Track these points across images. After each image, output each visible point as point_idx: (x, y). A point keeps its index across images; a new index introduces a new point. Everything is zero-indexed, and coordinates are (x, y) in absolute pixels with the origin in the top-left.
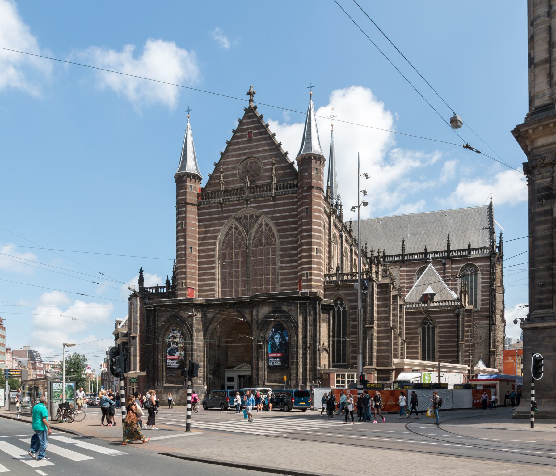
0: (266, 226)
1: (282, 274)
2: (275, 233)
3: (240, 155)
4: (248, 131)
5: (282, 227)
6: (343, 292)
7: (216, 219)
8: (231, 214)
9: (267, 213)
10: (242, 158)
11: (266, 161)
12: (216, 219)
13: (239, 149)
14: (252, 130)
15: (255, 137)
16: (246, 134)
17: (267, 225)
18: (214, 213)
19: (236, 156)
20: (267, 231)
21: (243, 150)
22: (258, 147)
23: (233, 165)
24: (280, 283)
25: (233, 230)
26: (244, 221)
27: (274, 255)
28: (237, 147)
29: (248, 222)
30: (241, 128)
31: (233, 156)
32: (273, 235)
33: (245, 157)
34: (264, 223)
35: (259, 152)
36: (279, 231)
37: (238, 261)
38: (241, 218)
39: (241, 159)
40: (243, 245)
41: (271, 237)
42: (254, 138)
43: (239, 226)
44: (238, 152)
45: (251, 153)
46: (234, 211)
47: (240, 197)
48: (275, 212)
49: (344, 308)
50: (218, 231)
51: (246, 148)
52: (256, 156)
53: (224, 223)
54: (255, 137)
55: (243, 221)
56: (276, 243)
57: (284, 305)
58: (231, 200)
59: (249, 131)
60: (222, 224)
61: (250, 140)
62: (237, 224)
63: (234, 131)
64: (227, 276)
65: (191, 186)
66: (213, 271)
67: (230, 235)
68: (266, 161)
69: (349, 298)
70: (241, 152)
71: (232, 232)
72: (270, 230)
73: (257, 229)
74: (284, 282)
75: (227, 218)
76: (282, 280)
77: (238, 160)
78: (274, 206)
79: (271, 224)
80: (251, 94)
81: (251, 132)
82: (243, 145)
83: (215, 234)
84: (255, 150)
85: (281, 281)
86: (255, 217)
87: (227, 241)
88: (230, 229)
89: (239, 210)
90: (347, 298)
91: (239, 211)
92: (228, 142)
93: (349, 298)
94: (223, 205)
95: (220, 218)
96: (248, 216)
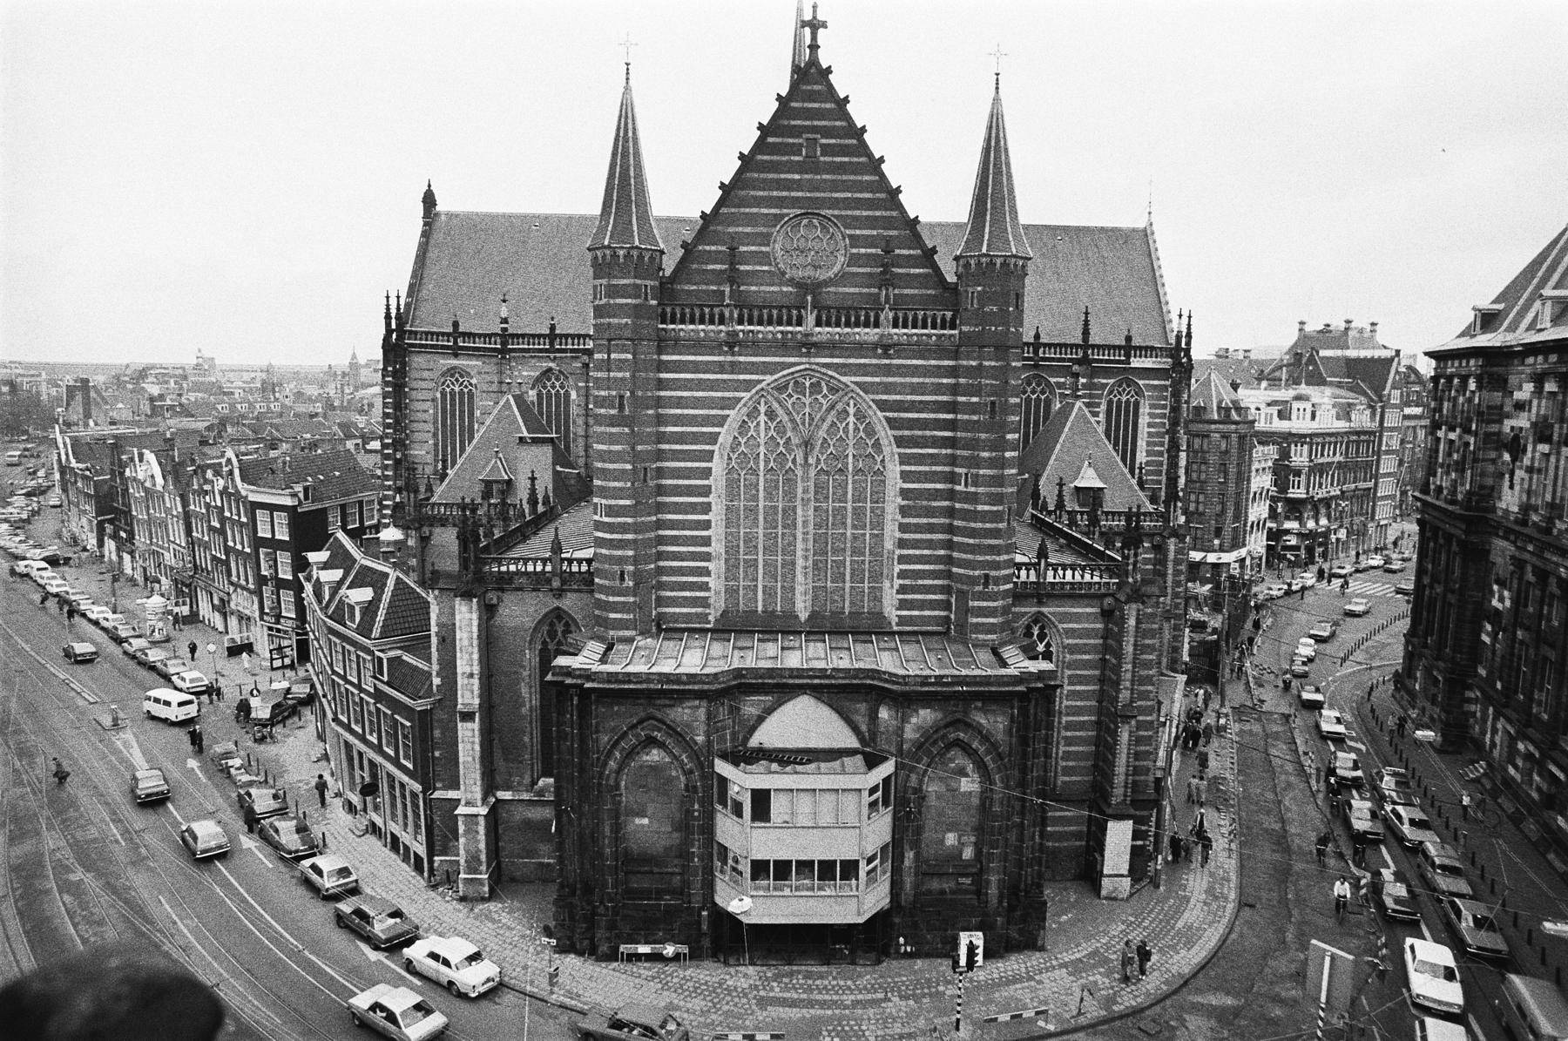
1: (902, 559)
2: (884, 442)
3: (780, 202)
5: (907, 433)
6: (1051, 609)
7: (713, 386)
8: (761, 377)
9: (866, 388)
10: (785, 211)
11: (858, 232)
12: (713, 386)
15: (827, 159)
16: (801, 145)
17: (860, 416)
20: (862, 434)
21: (789, 189)
22: (835, 186)
24: (898, 582)
25: (762, 418)
26: (793, 400)
27: (877, 502)
28: (771, 176)
31: (759, 202)
32: (877, 445)
34: (852, 410)
35: (835, 203)
37: (776, 508)
38: (786, 387)
39: (788, 215)
41: (870, 450)
42: (822, 159)
43: (780, 412)
47: (788, 332)
48: (888, 388)
49: (1048, 645)
50: (721, 420)
51: (798, 185)
52: (829, 212)
54: (827, 159)
55: (790, 396)
57: (976, 708)
59: (810, 136)
61: (811, 166)
62: (775, 405)
68: (858, 232)
69: (1065, 626)
70: (785, 194)
71: (758, 424)
72: (870, 432)
73: (833, 424)
74: (907, 582)
75: (748, 386)
76: (902, 575)
77: (775, 215)
78: (888, 370)
79: (878, 417)
80: (815, 25)
81: (815, 139)
83: (717, 429)
87: (743, 448)
88: (753, 413)
89: (783, 369)
90: (1060, 626)
91: (785, 372)
92: (742, 156)
93: (1065, 626)
94: (736, 349)
96: (808, 384)
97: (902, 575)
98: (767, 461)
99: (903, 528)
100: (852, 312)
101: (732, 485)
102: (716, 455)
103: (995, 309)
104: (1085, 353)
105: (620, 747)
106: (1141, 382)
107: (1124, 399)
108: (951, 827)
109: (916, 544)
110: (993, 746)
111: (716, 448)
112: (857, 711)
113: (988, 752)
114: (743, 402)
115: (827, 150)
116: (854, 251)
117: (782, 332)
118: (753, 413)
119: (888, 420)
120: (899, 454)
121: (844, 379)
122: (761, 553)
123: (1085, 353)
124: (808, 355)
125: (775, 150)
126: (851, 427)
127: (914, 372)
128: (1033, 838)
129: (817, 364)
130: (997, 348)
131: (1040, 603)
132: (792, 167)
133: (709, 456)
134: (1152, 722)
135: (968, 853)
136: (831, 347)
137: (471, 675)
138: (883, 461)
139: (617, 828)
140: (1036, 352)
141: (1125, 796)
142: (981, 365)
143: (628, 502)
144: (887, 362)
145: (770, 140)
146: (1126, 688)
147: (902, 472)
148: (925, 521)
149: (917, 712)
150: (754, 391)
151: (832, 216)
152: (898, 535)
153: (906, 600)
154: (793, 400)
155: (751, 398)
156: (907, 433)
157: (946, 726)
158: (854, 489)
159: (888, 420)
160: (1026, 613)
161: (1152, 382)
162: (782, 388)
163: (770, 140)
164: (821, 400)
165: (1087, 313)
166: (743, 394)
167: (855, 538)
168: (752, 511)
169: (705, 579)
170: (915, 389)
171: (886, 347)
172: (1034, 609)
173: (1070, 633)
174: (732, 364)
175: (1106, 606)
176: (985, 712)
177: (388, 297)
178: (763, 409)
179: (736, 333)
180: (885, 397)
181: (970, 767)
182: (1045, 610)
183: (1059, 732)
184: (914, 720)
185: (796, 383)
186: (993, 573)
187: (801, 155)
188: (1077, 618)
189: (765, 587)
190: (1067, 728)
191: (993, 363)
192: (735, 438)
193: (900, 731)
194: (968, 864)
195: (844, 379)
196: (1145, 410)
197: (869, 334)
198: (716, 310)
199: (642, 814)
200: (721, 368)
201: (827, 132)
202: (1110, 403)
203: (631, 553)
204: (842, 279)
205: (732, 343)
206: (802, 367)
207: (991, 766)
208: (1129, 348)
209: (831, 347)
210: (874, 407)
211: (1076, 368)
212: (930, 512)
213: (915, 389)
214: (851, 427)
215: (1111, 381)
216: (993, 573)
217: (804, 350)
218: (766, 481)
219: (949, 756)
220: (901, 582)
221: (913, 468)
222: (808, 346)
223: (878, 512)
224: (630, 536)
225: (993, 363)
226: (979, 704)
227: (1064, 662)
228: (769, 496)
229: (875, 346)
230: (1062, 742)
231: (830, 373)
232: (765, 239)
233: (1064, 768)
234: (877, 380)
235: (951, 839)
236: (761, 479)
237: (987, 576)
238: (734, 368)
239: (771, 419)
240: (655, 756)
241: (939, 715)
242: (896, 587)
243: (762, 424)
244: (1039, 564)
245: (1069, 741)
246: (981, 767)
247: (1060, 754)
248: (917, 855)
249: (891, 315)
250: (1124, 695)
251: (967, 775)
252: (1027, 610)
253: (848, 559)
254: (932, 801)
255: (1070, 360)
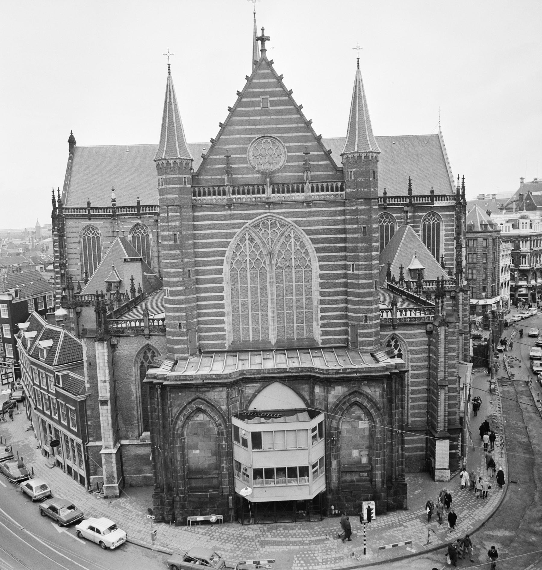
0: (296, 240)
1: (323, 310)
2: (310, 251)
3: (251, 131)
4: (261, 97)
5: (321, 245)
7: (220, 227)
8: (246, 221)
9: (299, 224)
11: (291, 144)
12: (220, 227)
13: (249, 123)
14: (268, 96)
16: (259, 102)
17: (297, 238)
18: (218, 218)
19: (245, 132)
21: (254, 125)
23: (242, 146)
24: (320, 322)
25: (247, 242)
26: (263, 231)
29: (270, 233)
30: (251, 90)
31: (239, 132)
32: (306, 252)
33: (260, 136)
34: (292, 235)
35: (278, 130)
36: (318, 250)
37: (256, 287)
39: (255, 138)
40: (263, 265)
41: (303, 255)
42: (271, 108)
43: (256, 238)
44: (248, 127)
45: (267, 129)
46: (249, 217)
47: (258, 198)
48: (310, 223)
49: (400, 350)
50: (226, 245)
51: (259, 122)
52: (275, 135)
53: (235, 233)
55: (261, 230)
56: (310, 264)
57: (364, 384)
58: (244, 200)
60: (231, 235)
63: (239, 93)
64: (240, 308)
65: (185, 178)
66: (221, 302)
67: (242, 249)
68: (291, 144)
69: (408, 340)
70: (253, 127)
71: (245, 245)
72: (303, 245)
73: (283, 243)
74: (325, 322)
75: (239, 226)
76: (323, 318)
78: (310, 214)
79: (306, 238)
80: (263, 39)
82: (255, 118)
84: (274, 126)
85: (321, 319)
86: (278, 226)
88: (242, 240)
89: (256, 217)
92: (230, 109)
93: (408, 340)
94: (232, 207)
95: (228, 226)
96: (269, 224)
97: (323, 318)
98: (251, 263)
99: (322, 294)
100: (290, 185)
101: (234, 278)
102: (225, 261)
103: (363, 180)
104: (410, 201)
105: (183, 414)
106: (440, 214)
107: (432, 223)
108: (356, 447)
109: (329, 302)
110: (375, 404)
111: (225, 258)
112: (303, 389)
113: (372, 407)
114: (237, 234)
115: (273, 103)
116: (289, 154)
117: (255, 198)
118: (242, 240)
119: (311, 239)
120: (318, 256)
121: (287, 220)
122: (250, 311)
123: (410, 201)
124: (269, 208)
125: (247, 104)
126: (293, 244)
127: (323, 214)
128: (398, 451)
129: (274, 213)
130: (365, 199)
131: (394, 329)
132: (255, 113)
133: (221, 263)
134: (456, 388)
135: (365, 460)
136: (281, 204)
137: (105, 382)
138: (310, 260)
139: (183, 456)
140: (385, 201)
141: (445, 427)
142: (357, 208)
143: (181, 288)
144: (309, 210)
145: (244, 100)
146: (442, 371)
147: (320, 266)
148: (333, 290)
149: (334, 388)
150: (242, 228)
151: (278, 137)
152: (320, 298)
153: (325, 331)
154: (263, 231)
155: (241, 232)
156: (321, 245)
157: (350, 395)
158: (296, 275)
159: (311, 239)
160: (387, 335)
161: (445, 213)
162: (256, 226)
163: (244, 100)
164: (277, 231)
165: (410, 180)
166: (237, 230)
167: (298, 301)
168: (245, 289)
169: (222, 326)
170: (324, 223)
171: (308, 203)
172: (392, 332)
173: (411, 344)
174: (231, 215)
175: (428, 329)
176: (369, 386)
177: (53, 191)
178: (247, 237)
179: (231, 200)
180: (309, 228)
181: (363, 416)
182: (397, 332)
183: (408, 396)
184: (333, 392)
185: (264, 223)
186: (369, 315)
187: (259, 106)
188: (414, 336)
189: (253, 328)
190: (412, 393)
191: (364, 207)
192: (234, 253)
193: (326, 399)
194: (364, 466)
195: (287, 220)
196: (442, 227)
197: (299, 196)
198: (221, 188)
199: (197, 448)
200: (225, 218)
201: (272, 94)
202: (424, 225)
203: (184, 314)
204: (284, 169)
205: (230, 205)
206: (266, 215)
207: (374, 414)
208: (433, 196)
209: (281, 204)
210: (304, 233)
211: (406, 208)
212: (335, 285)
213: (324, 223)
214: (293, 244)
215: (425, 214)
216: (369, 315)
217: (267, 206)
218: (251, 274)
219: (352, 410)
220: (323, 322)
221: (325, 263)
222: (269, 204)
223: (309, 287)
224: (183, 306)
225: (364, 207)
226: (366, 382)
227: (408, 359)
228: (253, 281)
229: (303, 202)
230: (410, 401)
231: (280, 217)
232: (244, 151)
233: (411, 414)
234: (304, 219)
235: (355, 453)
236: (248, 273)
237: (366, 317)
238: (232, 217)
239: (251, 242)
240: (201, 417)
241: (346, 389)
242: (320, 324)
243: (247, 245)
244: (392, 309)
245: (414, 400)
246: (369, 414)
247: (409, 407)
248: (338, 462)
249: (310, 186)
250: (441, 375)
251: (362, 420)
252: (388, 333)
253: (295, 312)
254: (344, 434)
255: (403, 204)
